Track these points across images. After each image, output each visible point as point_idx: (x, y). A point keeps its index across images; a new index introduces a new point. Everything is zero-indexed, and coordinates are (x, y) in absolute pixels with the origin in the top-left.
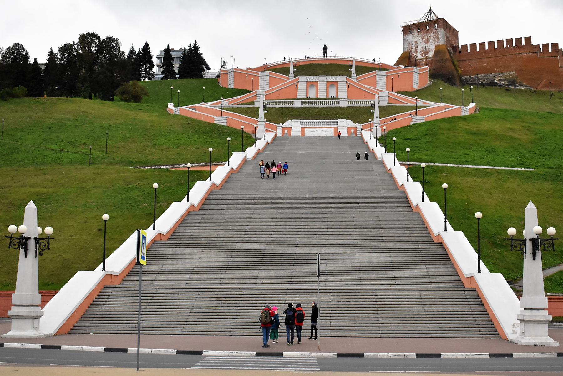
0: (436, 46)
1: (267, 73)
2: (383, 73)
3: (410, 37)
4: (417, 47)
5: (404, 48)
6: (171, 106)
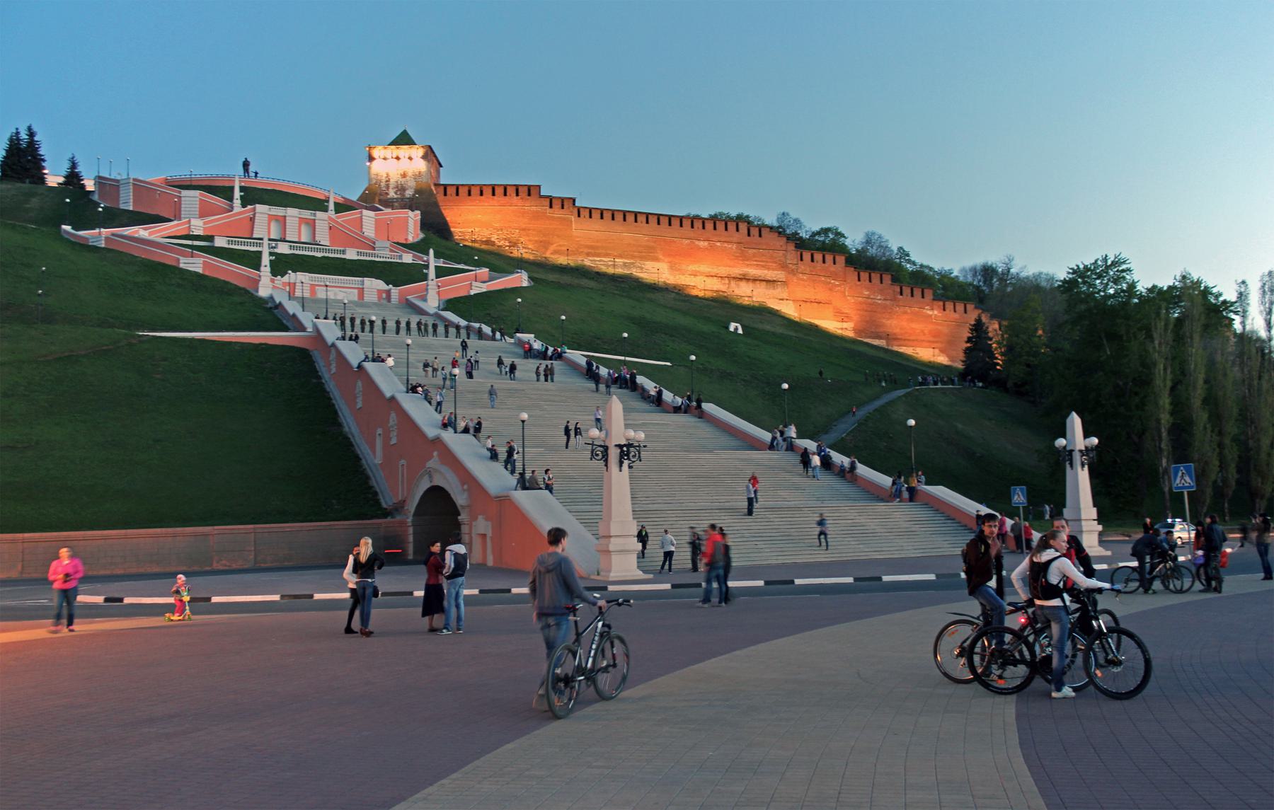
1: (197, 193)
6: (67, 228)
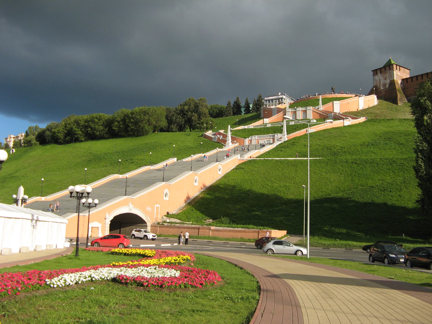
0: (390, 81)
2: (338, 102)
3: (376, 77)
4: (380, 83)
5: (374, 84)
